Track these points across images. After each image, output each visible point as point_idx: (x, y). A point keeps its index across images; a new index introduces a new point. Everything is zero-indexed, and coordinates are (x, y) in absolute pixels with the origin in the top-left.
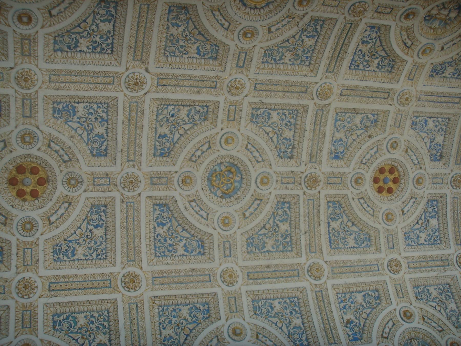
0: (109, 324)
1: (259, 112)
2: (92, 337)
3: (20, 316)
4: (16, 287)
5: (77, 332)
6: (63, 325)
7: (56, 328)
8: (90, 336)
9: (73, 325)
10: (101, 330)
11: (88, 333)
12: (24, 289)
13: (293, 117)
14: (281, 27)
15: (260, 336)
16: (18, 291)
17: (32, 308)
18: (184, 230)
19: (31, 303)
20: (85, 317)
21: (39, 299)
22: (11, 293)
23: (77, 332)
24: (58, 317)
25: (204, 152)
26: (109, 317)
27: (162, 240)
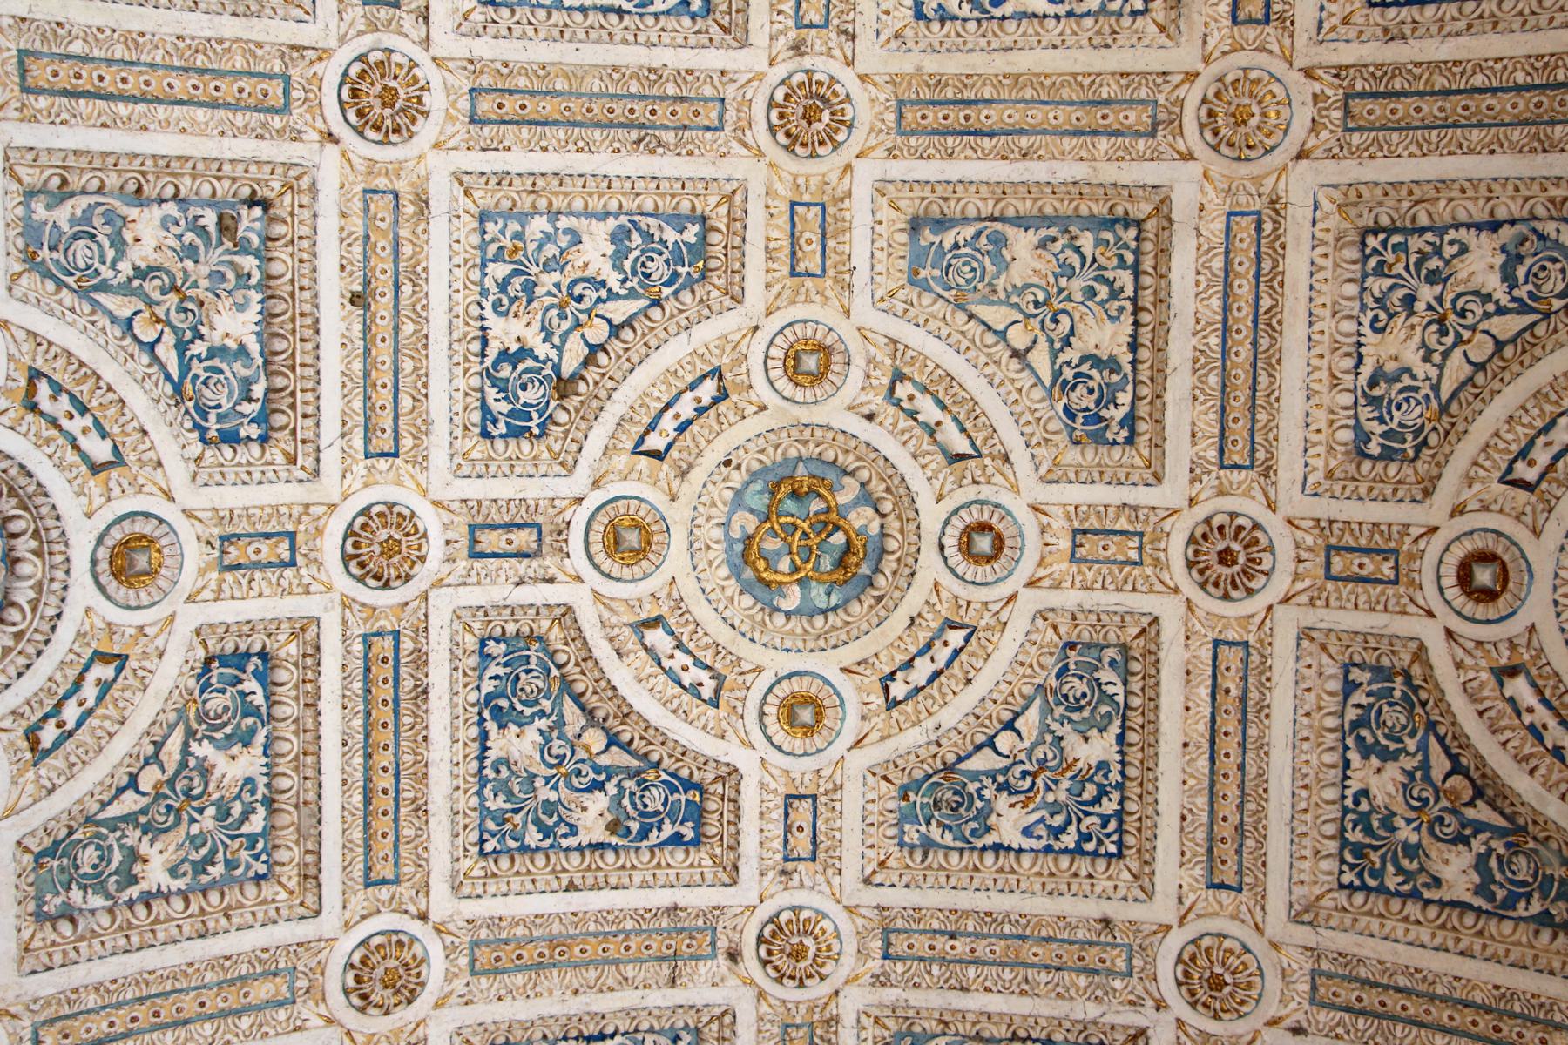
1: (1106, 675)
13: (1089, 838)
14: (1527, 719)
15: (107, 672)
18: (595, 349)
25: (932, 433)
27: (550, 250)
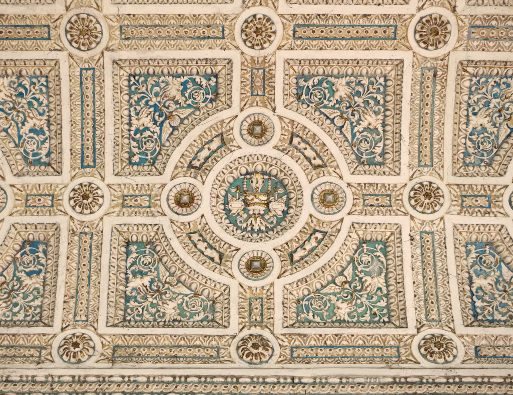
0: (384, 99)
2: (357, 117)
3: (248, 76)
4: (243, 31)
5: (333, 107)
6: (312, 93)
7: (302, 98)
8: (353, 115)
9: (328, 95)
10: (372, 108)
11: (350, 110)
12: (254, 35)
16: (244, 37)
17: (267, 65)
19: (265, 58)
20: (348, 84)
21: (278, 52)
22: (234, 40)
23: (333, 107)
24: (305, 81)
26: (386, 86)
